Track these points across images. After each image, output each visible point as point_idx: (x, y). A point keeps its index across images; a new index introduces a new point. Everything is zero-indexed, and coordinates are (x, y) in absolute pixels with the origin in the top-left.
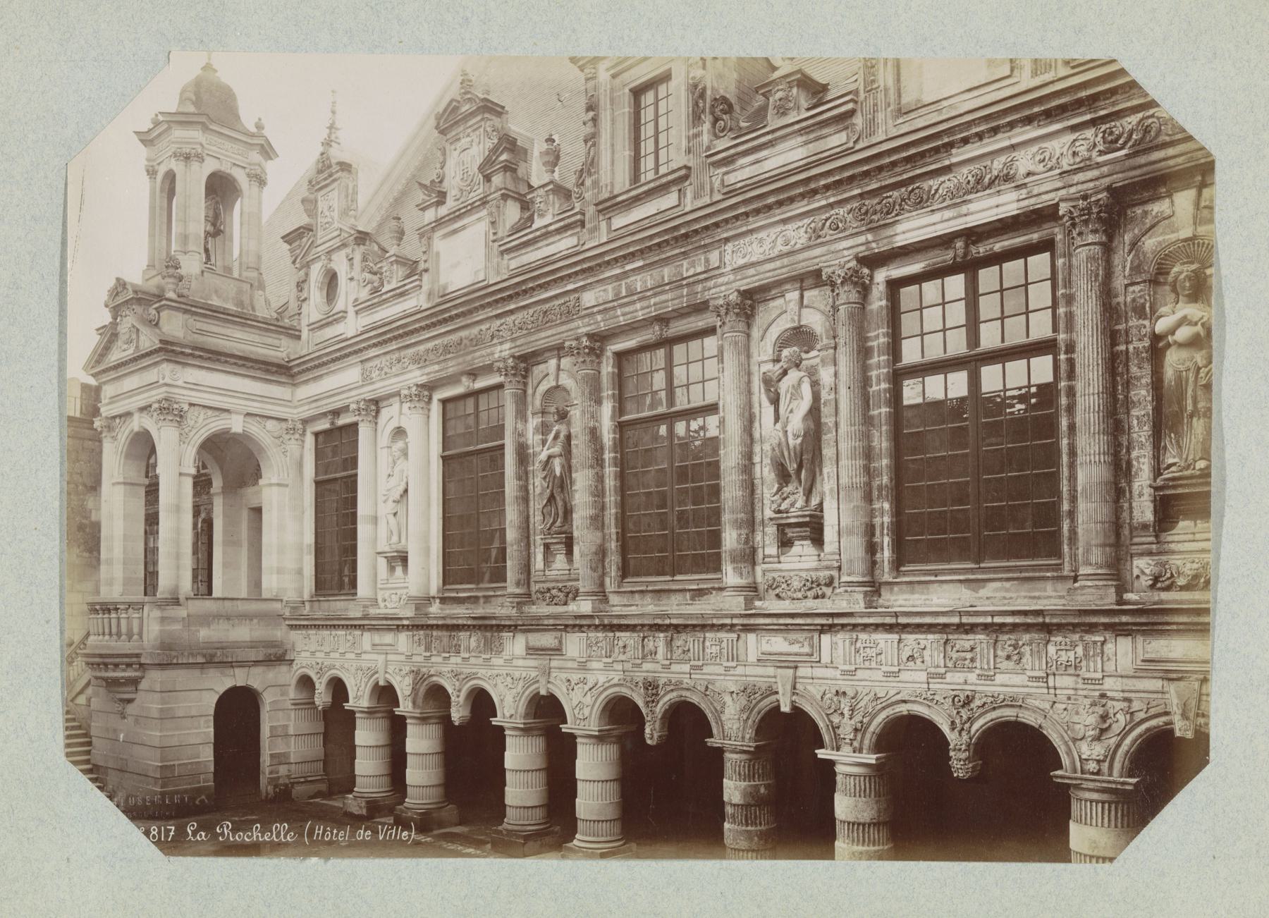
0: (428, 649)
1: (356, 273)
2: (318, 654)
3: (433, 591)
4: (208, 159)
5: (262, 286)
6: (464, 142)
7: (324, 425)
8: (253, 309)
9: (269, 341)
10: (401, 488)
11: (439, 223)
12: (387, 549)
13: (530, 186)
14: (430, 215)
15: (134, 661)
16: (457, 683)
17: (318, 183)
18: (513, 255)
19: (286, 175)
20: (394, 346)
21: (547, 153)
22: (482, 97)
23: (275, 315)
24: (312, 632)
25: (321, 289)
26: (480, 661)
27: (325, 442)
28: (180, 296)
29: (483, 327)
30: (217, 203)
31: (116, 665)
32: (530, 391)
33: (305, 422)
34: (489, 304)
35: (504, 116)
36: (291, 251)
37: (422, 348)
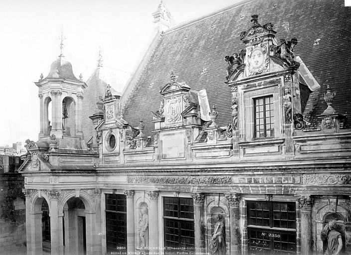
9: (88, 160)
10: (146, 225)
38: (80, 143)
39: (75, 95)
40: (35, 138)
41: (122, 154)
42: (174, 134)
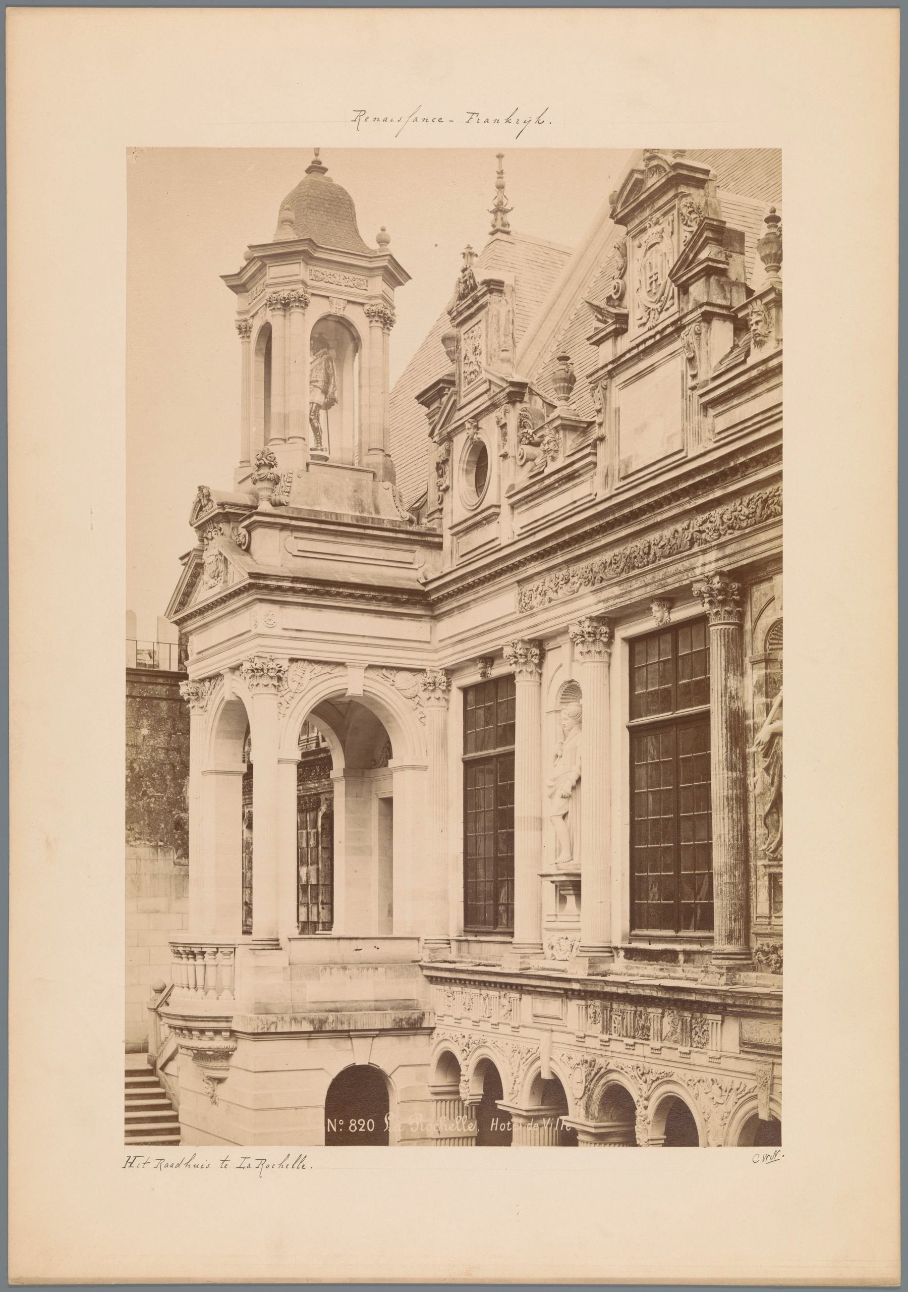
0: (606, 1029)
1: (511, 447)
2: (468, 1022)
3: (617, 942)
4: (313, 301)
5: (390, 475)
6: (650, 236)
7: (473, 677)
8: (377, 511)
11: (618, 365)
12: (553, 871)
13: (749, 292)
14: (607, 352)
15: (222, 1026)
16: (645, 1087)
17: (460, 313)
18: (720, 409)
19: (423, 307)
20: (559, 559)
21: (767, 242)
22: (672, 161)
23: (407, 515)
24: (457, 989)
25: (467, 472)
26: (675, 1055)
27: (477, 702)
28: (276, 505)
29: (679, 527)
30: (329, 359)
31: (202, 1031)
32: (748, 626)
33: (450, 672)
34: (685, 492)
35: (710, 186)
36: (430, 416)
37: (597, 560)
38: (374, 492)
39: (359, 309)
40: (228, 488)
41: (505, 510)
42: (652, 369)
